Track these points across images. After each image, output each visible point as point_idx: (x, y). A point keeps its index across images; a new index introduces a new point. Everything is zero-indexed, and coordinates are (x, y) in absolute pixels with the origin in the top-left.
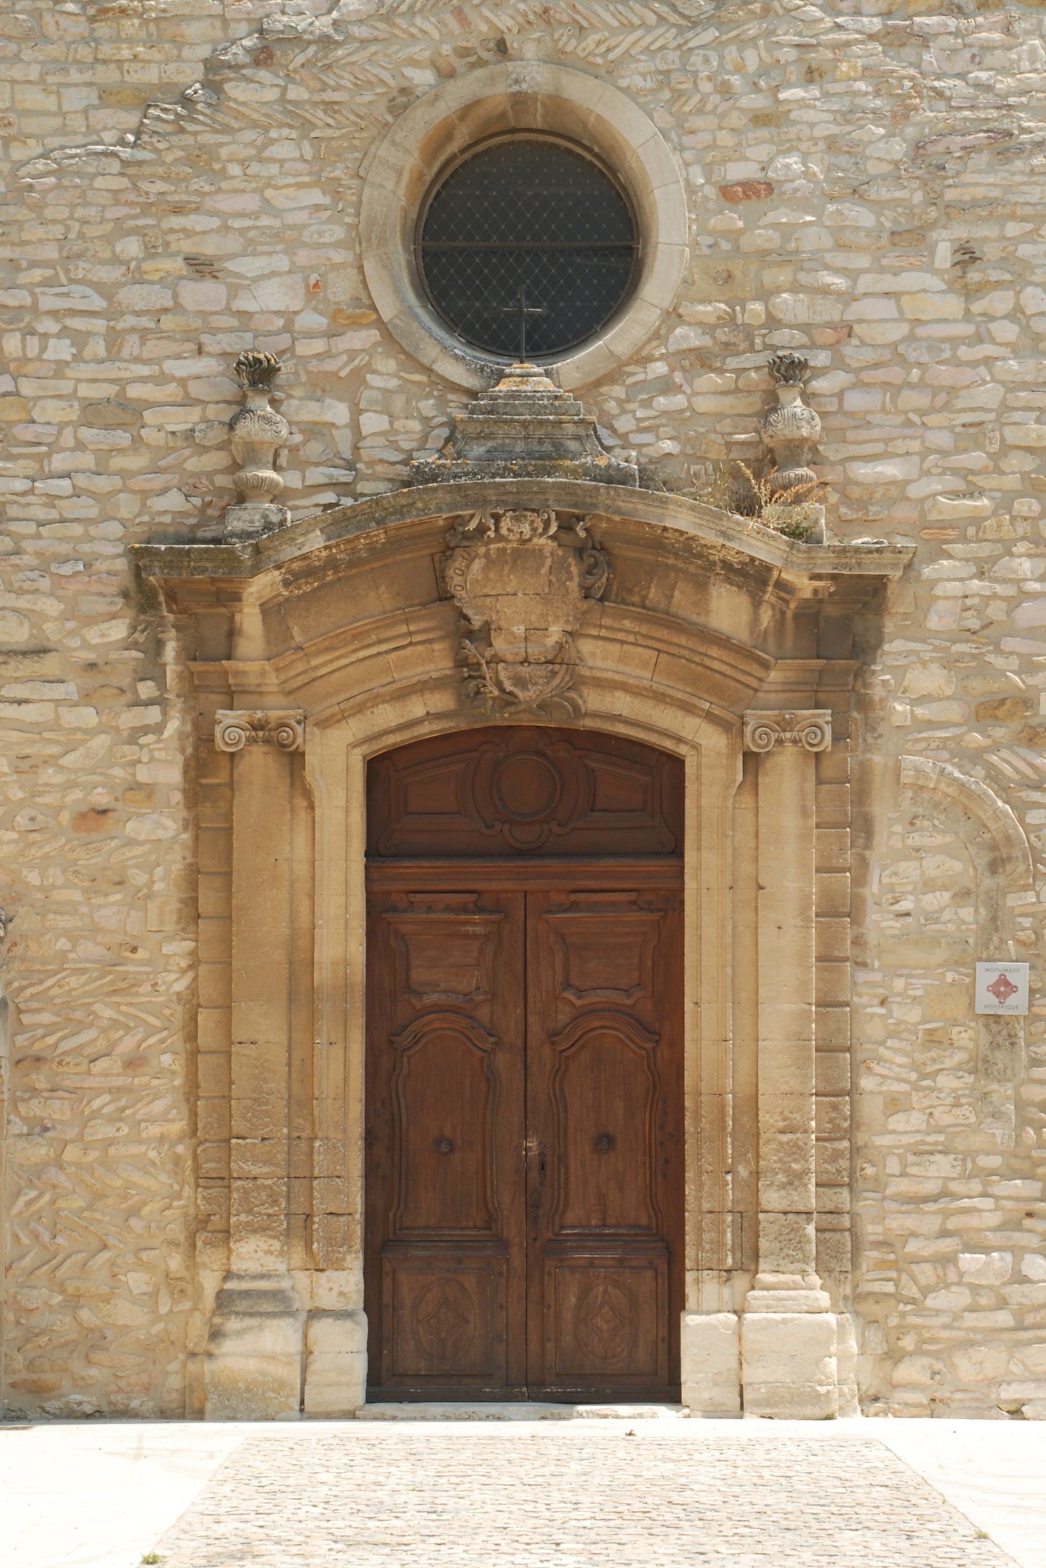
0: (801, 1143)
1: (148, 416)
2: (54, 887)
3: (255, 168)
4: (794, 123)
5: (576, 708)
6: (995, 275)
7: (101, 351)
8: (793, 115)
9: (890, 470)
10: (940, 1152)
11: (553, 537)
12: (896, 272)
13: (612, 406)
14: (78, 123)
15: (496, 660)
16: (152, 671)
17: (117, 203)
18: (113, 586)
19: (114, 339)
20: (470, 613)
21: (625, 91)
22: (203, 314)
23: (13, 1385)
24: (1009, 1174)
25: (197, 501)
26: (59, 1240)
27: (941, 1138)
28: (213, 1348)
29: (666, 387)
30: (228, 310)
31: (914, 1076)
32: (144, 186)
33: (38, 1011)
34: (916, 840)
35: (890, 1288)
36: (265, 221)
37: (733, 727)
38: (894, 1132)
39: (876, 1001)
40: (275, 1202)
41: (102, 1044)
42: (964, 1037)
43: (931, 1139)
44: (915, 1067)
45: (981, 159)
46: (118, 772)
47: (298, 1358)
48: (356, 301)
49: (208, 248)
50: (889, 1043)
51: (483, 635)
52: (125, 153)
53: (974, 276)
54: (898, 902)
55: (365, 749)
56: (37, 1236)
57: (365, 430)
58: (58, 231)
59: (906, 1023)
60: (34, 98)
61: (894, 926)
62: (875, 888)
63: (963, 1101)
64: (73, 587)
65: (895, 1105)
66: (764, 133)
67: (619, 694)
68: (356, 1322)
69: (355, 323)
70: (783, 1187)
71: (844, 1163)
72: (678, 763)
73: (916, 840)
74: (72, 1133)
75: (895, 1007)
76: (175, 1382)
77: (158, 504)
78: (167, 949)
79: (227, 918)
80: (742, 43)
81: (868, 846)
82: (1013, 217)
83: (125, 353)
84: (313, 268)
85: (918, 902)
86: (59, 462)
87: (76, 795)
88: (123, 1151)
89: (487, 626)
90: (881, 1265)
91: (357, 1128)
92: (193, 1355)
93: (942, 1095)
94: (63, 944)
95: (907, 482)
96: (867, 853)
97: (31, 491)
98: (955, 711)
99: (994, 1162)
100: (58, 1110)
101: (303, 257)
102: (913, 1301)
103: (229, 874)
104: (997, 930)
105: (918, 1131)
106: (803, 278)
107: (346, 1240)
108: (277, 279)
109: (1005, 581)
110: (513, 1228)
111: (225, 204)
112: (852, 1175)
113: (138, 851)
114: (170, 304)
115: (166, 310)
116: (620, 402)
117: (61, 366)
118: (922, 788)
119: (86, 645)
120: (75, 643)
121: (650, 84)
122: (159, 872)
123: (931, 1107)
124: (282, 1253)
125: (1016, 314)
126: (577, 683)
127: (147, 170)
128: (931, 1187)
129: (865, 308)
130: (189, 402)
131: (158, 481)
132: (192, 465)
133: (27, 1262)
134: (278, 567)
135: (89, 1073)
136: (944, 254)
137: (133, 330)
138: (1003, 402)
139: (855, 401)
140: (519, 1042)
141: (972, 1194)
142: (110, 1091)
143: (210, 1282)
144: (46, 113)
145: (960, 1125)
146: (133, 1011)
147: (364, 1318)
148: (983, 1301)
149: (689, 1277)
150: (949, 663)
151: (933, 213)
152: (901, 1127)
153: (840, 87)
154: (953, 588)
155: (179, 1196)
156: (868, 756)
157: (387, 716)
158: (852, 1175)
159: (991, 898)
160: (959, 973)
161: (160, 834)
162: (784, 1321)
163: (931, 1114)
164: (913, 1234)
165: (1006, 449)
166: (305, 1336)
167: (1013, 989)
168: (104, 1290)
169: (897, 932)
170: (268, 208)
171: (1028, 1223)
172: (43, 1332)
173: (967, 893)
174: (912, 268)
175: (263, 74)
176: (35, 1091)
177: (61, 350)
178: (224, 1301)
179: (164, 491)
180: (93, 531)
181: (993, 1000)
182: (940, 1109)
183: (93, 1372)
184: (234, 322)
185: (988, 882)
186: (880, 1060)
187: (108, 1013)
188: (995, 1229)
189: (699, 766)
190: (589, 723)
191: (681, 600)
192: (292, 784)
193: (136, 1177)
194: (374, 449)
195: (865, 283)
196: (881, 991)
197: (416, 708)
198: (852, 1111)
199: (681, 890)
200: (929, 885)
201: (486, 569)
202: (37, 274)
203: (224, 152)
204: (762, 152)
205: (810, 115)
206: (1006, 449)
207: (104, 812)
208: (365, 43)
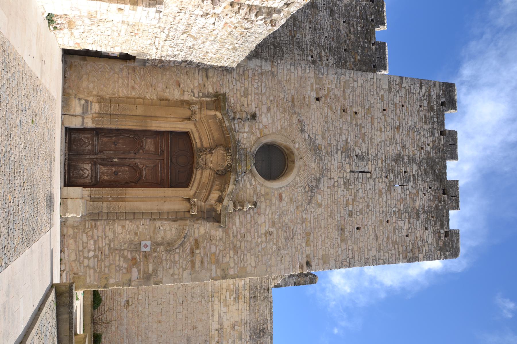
1: (246, 99)
2: (166, 76)
3: (283, 118)
4: (290, 205)
5: (197, 169)
6: (268, 238)
7: (255, 92)
8: (292, 205)
9: (238, 223)
11: (227, 165)
12: (269, 222)
13: (248, 175)
14: (289, 91)
15: (206, 154)
16: (205, 96)
17: (278, 96)
18: (218, 90)
19: (257, 94)
20: (214, 150)
21: (295, 178)
22: (262, 109)
23: (72, 62)
24: (110, 248)
25: (232, 105)
26: (100, 72)
27: (117, 236)
28: (77, 99)
29: (251, 185)
30: (262, 113)
31: (129, 230)
32: (281, 101)
33: (143, 71)
34: (173, 229)
35: (87, 227)
36: (276, 119)
37: (194, 196)
38: (118, 227)
40: (106, 111)
41: (137, 82)
42: (137, 239)
43: (117, 234)
44: (131, 230)
45: (285, 235)
46: (186, 88)
47: (74, 114)
48: (264, 134)
49: (272, 110)
51: (211, 152)
52: (285, 98)
53: (268, 235)
55: (190, 132)
56: (101, 68)
57: (244, 134)
58: (274, 87)
60: (292, 85)
61: (157, 225)
62: (164, 222)
64: (218, 84)
65: (123, 227)
66: (289, 199)
67: (200, 176)
68: (81, 126)
69: (261, 133)
70: (107, 206)
71: (112, 218)
72: (187, 187)
73: (173, 229)
74: (120, 76)
76: (71, 91)
77: (232, 99)
78: (154, 95)
79: (160, 105)
80: (302, 196)
81: (172, 221)
82: (277, 241)
83: (255, 96)
84: (269, 127)
85: (162, 230)
86: (238, 83)
87: (183, 81)
88: (117, 85)
89: (212, 153)
90: (92, 225)
91: (120, 127)
92: (76, 95)
94: (156, 77)
95: (235, 225)
97: (234, 78)
98: (196, 235)
99: (112, 246)
100: (125, 73)
101: (270, 125)
102: (84, 231)
103: (168, 106)
106: (268, 207)
107: (98, 124)
108: (267, 121)
109: (219, 243)
110: (100, 157)
111: (278, 113)
112: (110, 219)
113: (172, 91)
114: (263, 103)
115: (262, 103)
116: (248, 177)
117: (253, 85)
119: (208, 85)
120: (209, 83)
122: (169, 94)
124: (95, 112)
125: (262, 242)
126: (202, 169)
127: (283, 102)
128: (107, 234)
129: (263, 217)
130: (248, 105)
131: (235, 99)
132: (238, 105)
133: (96, 66)
134: (222, 117)
135: (132, 80)
136: (271, 230)
138: (248, 241)
139: (249, 216)
140: (136, 158)
142: (128, 83)
143: (90, 99)
144: (290, 87)
146: (143, 88)
147: (82, 127)
148: (84, 244)
149: (89, 189)
150: (205, 234)
151: (278, 227)
152: (119, 228)
153: (295, 212)
154: (217, 234)
155: (107, 94)
157: (196, 135)
158: (110, 219)
161: (175, 95)
162: (80, 207)
164: (98, 231)
165: (241, 242)
166: (79, 116)
167: (146, 248)
168: (90, 80)
170: (278, 120)
171: (100, 252)
172: (82, 68)
173: (163, 239)
174: (269, 225)
175: (297, 121)
176: (128, 70)
177: (256, 86)
178: (87, 101)
179: (234, 100)
180: (227, 88)
181: (143, 244)
183: (74, 77)
184: (260, 114)
185: (165, 242)
186: (132, 224)
187: (143, 84)
188: (99, 247)
189: (187, 191)
190: (195, 171)
191: (216, 187)
192: (184, 118)
193: (111, 87)
194: (241, 135)
195: (267, 217)
197: (198, 141)
199: (164, 187)
200: (165, 232)
201: (222, 153)
202: (267, 83)
203: (286, 114)
204: (286, 200)
205: (292, 207)
206: (241, 242)
207: (179, 86)
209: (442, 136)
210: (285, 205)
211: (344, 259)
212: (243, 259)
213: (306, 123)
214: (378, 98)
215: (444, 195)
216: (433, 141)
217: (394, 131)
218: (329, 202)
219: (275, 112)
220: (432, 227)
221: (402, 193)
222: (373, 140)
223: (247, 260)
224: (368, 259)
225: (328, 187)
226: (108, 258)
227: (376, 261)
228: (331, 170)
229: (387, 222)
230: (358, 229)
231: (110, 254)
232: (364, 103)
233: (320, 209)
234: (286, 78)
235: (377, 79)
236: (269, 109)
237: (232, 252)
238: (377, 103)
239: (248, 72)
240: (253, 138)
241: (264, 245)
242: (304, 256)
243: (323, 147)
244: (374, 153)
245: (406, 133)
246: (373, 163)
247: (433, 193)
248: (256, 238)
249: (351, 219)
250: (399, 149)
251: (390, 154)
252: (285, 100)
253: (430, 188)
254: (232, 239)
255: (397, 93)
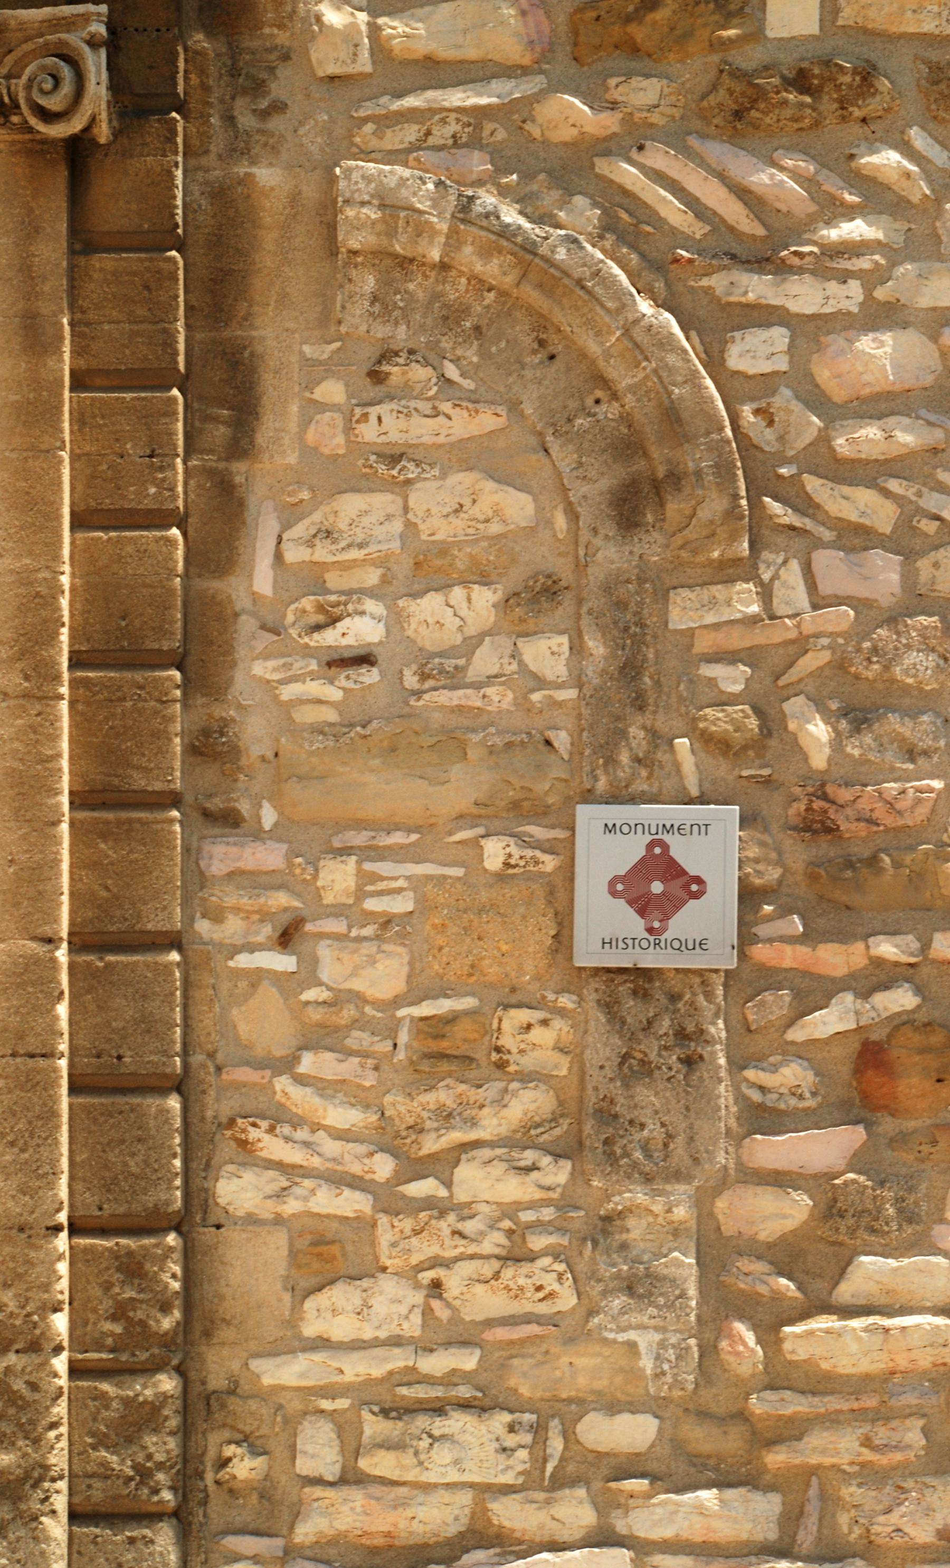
0: (18, 1385)
10: (465, 1405)
27: (469, 1361)
38: (322, 1343)
39: (266, 932)
50: (308, 1063)
54: (334, 621)
59: (359, 998)
63: (537, 1242)
75: (324, 951)
93: (469, 1227)
96: (239, 468)
104: (640, 703)
105: (396, 1342)
118: (405, 263)
123: (436, 1262)
141: (565, 1535)
145: (528, 1319)
156: (242, 169)
159: (621, 605)
160: (524, 841)
163: (436, 1285)
169: (331, 716)
182: (467, 1268)
196: (280, 900)
198: (188, 1278)
226: (830, 1502)
231: (776, 1458)
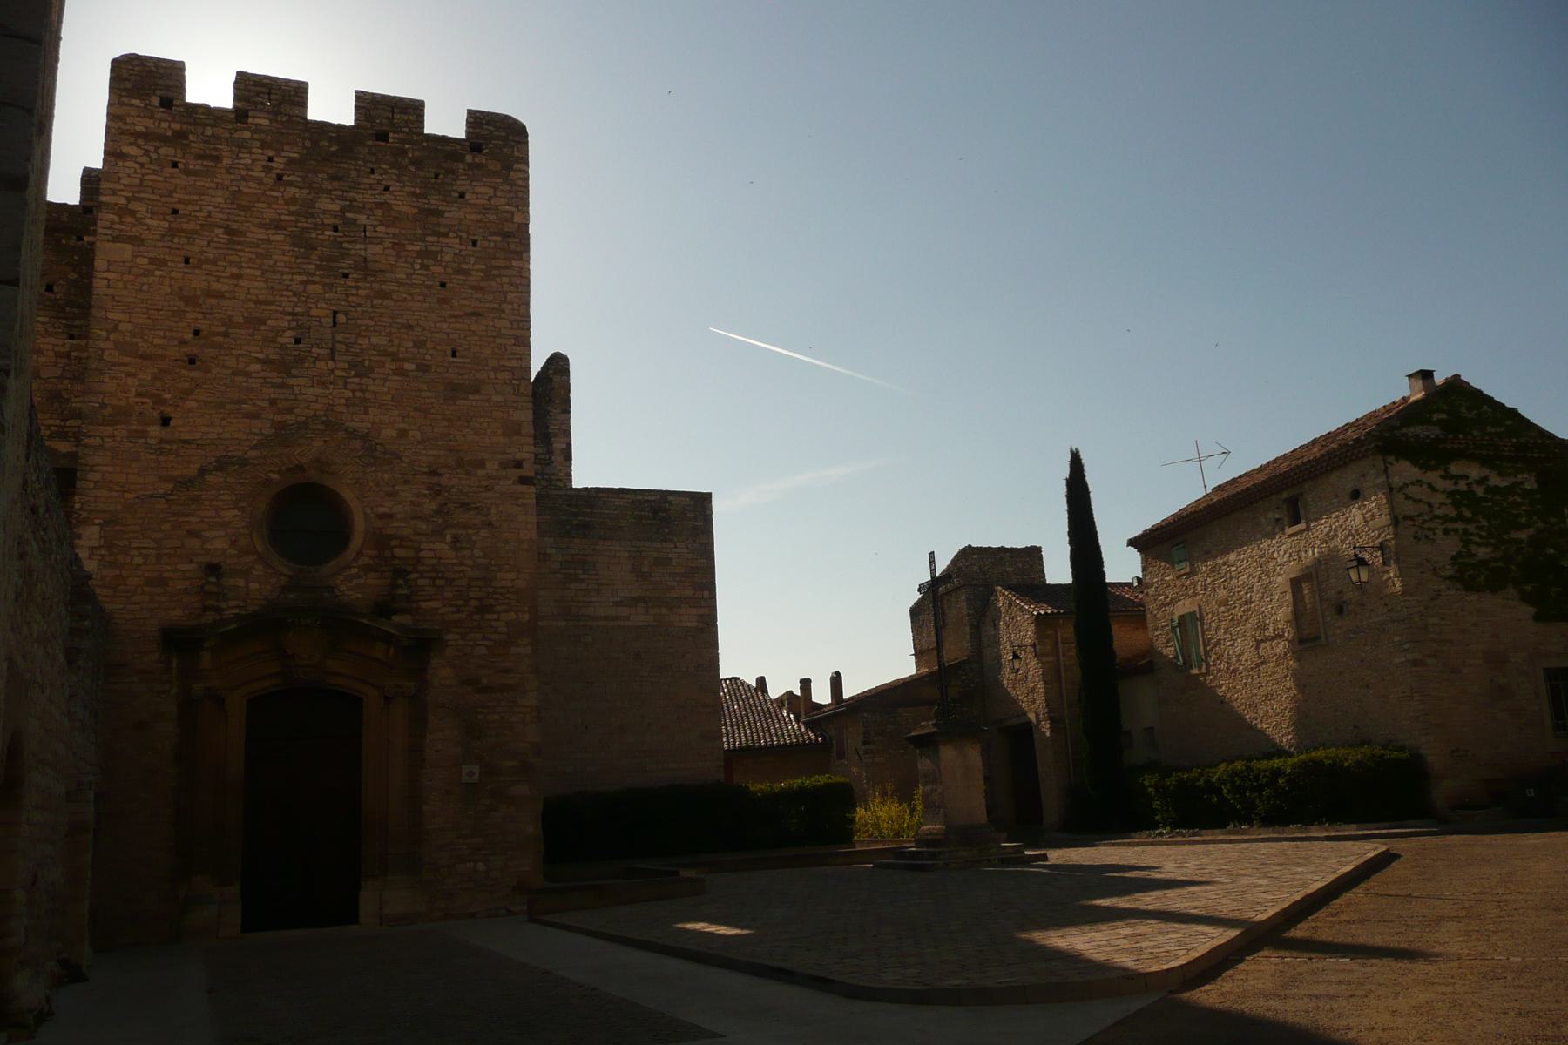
3: (214, 503)
6: (464, 545)
36: (217, 520)
52: (167, 497)
53: (458, 545)
58: (141, 521)
95: (438, 609)
115: (178, 548)
117: (138, 566)
121: (353, 482)
136: (448, 538)
137: (166, 554)
144: (141, 484)
175: (219, 473)
208: (255, 465)
209: (250, 120)
210: (400, 506)
211: (514, 391)
212: (502, 594)
213: (225, 454)
214: (158, 273)
215: (390, 140)
216: (262, 147)
217: (239, 243)
218: (396, 412)
219: (199, 519)
220: (459, 182)
221: (381, 243)
222: (261, 298)
223: (503, 587)
224: (516, 338)
225: (366, 413)
227: (522, 321)
228: (329, 404)
229: (443, 285)
230: (454, 355)
232: (174, 311)
233: (411, 433)
234: (118, 491)
235: (108, 271)
236: (193, 534)
237: (488, 616)
238: (171, 278)
239: (106, 576)
240: (258, 570)
241: (478, 553)
242: (503, 473)
243: (278, 418)
244: (292, 299)
245: (242, 213)
246: (313, 306)
247: (384, 166)
248: (463, 568)
249: (433, 368)
250: (280, 238)
251: (293, 260)
252: (172, 497)
253: (372, 172)
254: (463, 616)
255: (142, 224)
